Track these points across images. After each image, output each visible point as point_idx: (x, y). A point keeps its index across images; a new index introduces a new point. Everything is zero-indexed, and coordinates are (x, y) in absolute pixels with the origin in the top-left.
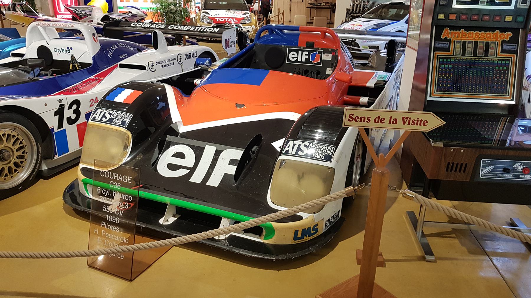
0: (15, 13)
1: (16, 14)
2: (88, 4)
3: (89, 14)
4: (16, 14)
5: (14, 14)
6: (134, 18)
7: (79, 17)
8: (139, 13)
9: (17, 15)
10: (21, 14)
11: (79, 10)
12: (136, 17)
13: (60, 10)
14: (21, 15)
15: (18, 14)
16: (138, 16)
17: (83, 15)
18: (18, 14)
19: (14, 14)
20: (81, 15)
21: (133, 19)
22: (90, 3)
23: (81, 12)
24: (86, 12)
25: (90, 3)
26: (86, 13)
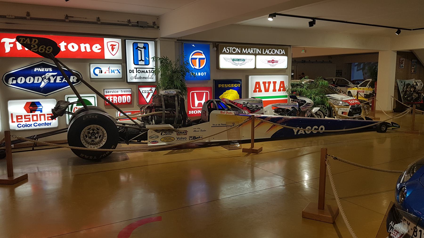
0: (224, 113)
1: (225, 113)
2: (220, 97)
3: (260, 107)
4: (225, 113)
5: (223, 114)
6: (307, 107)
7: (251, 110)
8: (311, 102)
9: (227, 114)
10: (232, 113)
11: (248, 103)
12: (309, 105)
13: (194, 105)
14: (232, 114)
15: (228, 113)
16: (310, 105)
17: (255, 108)
18: (228, 113)
19: (223, 114)
20: (253, 109)
21: (306, 108)
22: (223, 95)
23: (251, 105)
24: (257, 105)
25: (222, 95)
26: (256, 106)
